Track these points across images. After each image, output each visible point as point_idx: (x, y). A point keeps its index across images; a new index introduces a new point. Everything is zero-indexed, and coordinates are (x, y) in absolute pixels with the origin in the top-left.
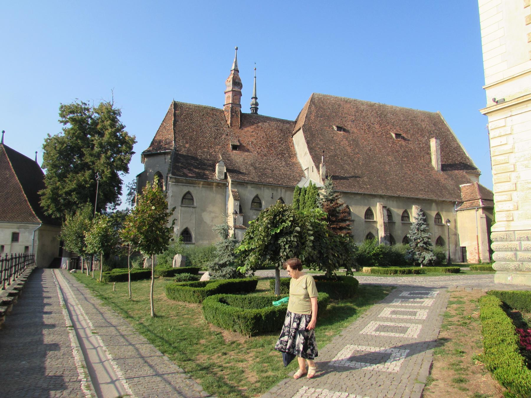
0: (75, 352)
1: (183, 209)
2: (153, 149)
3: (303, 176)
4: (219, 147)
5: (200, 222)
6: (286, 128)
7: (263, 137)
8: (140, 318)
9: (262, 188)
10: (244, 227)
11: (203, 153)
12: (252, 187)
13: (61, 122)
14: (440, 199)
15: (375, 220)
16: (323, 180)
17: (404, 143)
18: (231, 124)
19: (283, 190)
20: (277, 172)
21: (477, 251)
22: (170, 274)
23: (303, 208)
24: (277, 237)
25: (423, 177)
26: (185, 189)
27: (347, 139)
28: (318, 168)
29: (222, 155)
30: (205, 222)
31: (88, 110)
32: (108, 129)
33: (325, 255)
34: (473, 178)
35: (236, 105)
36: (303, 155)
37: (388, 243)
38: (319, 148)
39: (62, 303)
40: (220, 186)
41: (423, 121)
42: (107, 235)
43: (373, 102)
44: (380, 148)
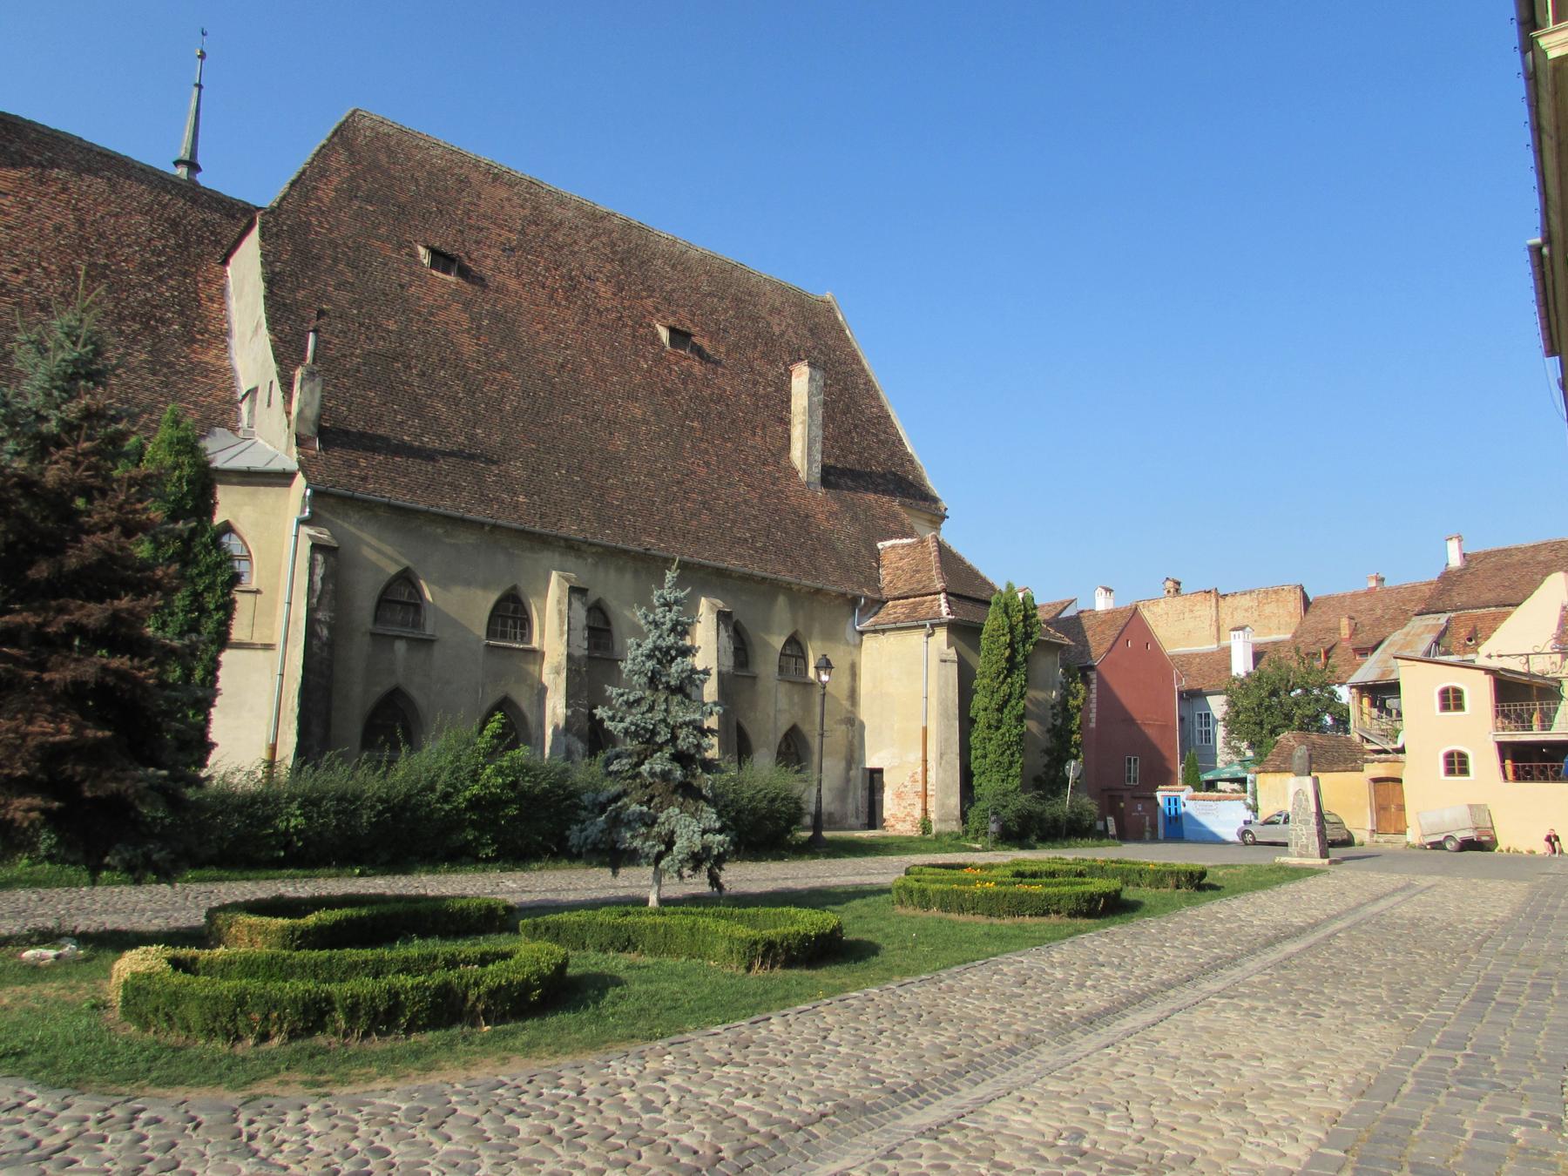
3: (223, 425)
6: (198, 222)
14: (805, 582)
15: (535, 644)
16: (301, 441)
17: (698, 369)
21: (919, 788)
25: (753, 497)
27: (467, 306)
28: (287, 386)
34: (921, 527)
36: (249, 334)
37: (580, 746)
41: (774, 311)
43: (604, 207)
44: (604, 366)
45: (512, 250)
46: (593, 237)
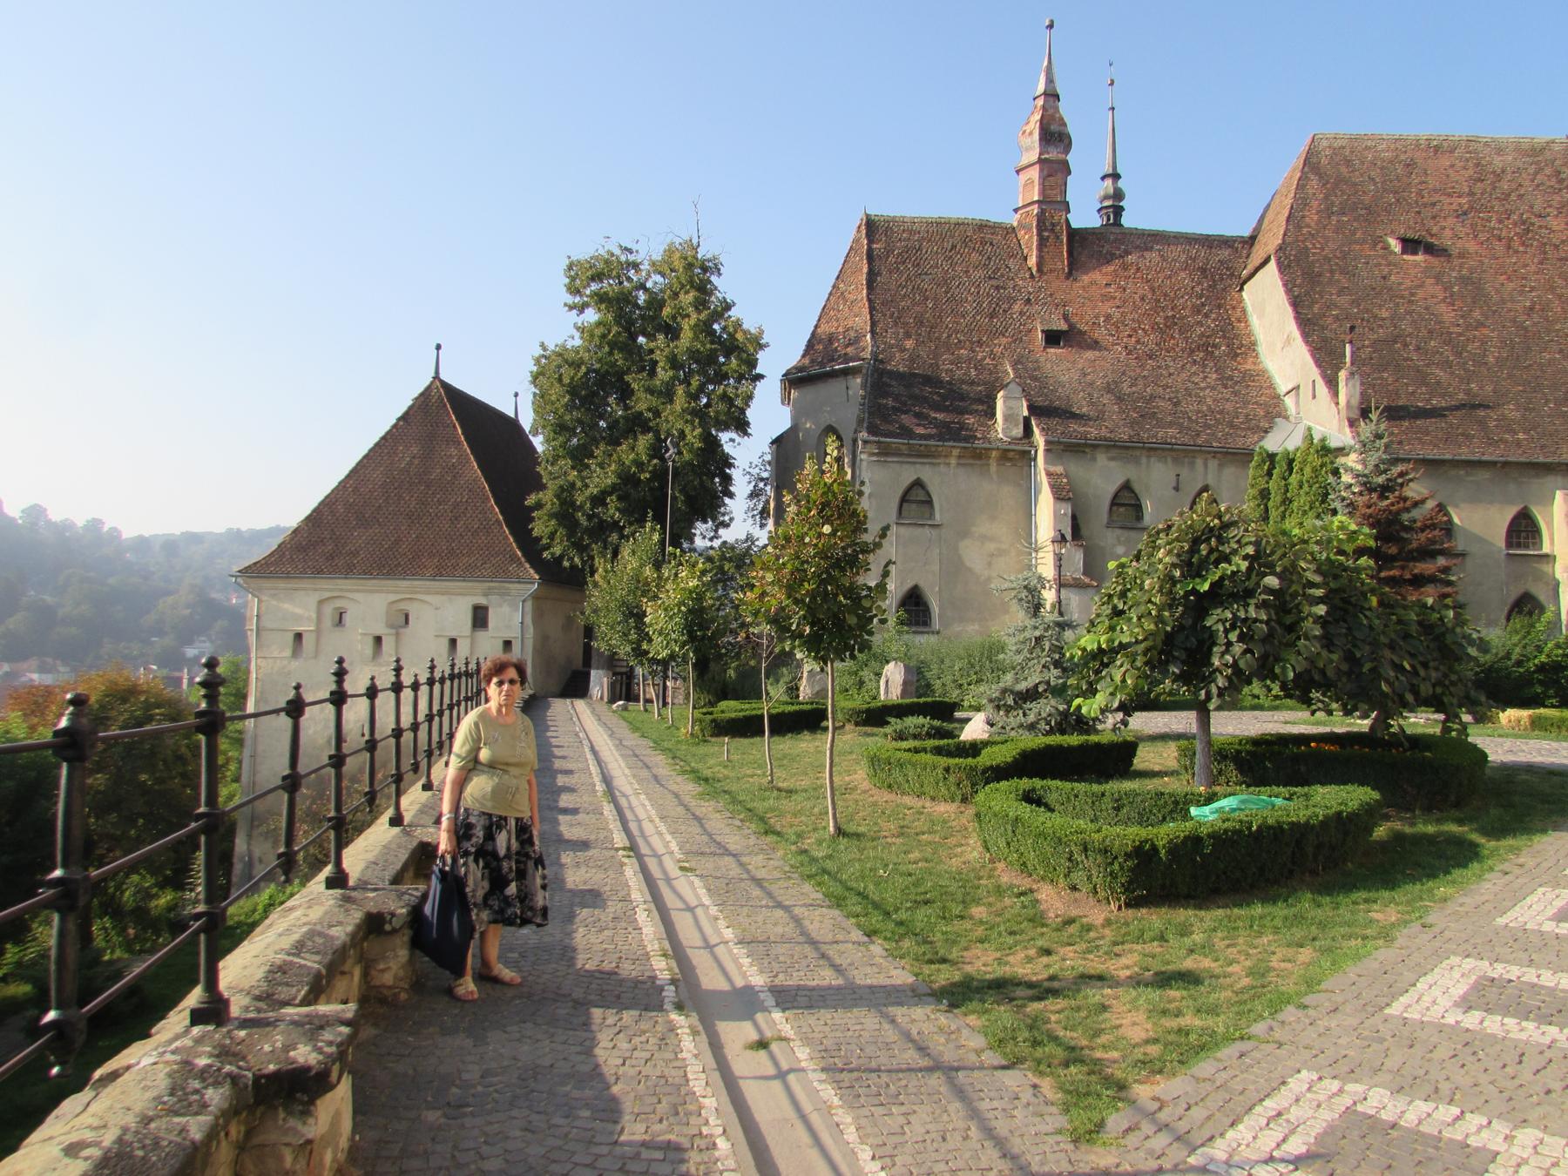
0: (641, 916)
1: (902, 530)
2: (812, 361)
4: (1004, 340)
5: (955, 569)
6: (1219, 263)
7: (1142, 299)
8: (800, 836)
9: (1144, 460)
10: (1087, 580)
11: (957, 362)
12: (1112, 459)
13: (571, 308)
15: (1546, 549)
16: (1352, 423)
18: (1040, 265)
19: (1213, 464)
20: (1190, 407)
22: (875, 717)
23: (1283, 518)
24: (1200, 605)
26: (907, 474)
27: (1438, 278)
28: (1332, 384)
29: (1014, 365)
30: (970, 570)
31: (636, 266)
32: (688, 316)
33: (1367, 667)
35: (1052, 202)
36: (1279, 346)
38: (1337, 318)
39: (600, 787)
40: (1010, 460)
42: (702, 610)
45: (1465, 213)
46: (1536, 174)
